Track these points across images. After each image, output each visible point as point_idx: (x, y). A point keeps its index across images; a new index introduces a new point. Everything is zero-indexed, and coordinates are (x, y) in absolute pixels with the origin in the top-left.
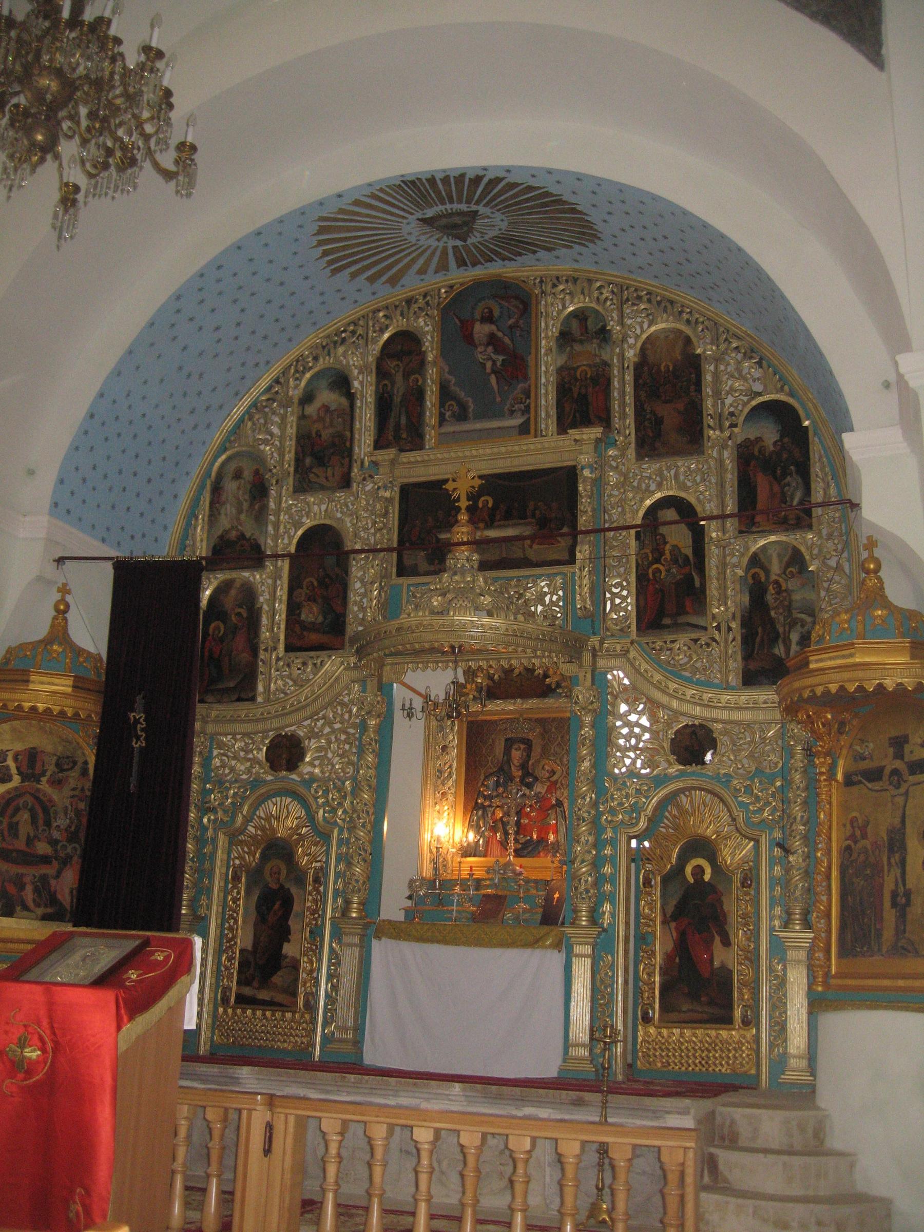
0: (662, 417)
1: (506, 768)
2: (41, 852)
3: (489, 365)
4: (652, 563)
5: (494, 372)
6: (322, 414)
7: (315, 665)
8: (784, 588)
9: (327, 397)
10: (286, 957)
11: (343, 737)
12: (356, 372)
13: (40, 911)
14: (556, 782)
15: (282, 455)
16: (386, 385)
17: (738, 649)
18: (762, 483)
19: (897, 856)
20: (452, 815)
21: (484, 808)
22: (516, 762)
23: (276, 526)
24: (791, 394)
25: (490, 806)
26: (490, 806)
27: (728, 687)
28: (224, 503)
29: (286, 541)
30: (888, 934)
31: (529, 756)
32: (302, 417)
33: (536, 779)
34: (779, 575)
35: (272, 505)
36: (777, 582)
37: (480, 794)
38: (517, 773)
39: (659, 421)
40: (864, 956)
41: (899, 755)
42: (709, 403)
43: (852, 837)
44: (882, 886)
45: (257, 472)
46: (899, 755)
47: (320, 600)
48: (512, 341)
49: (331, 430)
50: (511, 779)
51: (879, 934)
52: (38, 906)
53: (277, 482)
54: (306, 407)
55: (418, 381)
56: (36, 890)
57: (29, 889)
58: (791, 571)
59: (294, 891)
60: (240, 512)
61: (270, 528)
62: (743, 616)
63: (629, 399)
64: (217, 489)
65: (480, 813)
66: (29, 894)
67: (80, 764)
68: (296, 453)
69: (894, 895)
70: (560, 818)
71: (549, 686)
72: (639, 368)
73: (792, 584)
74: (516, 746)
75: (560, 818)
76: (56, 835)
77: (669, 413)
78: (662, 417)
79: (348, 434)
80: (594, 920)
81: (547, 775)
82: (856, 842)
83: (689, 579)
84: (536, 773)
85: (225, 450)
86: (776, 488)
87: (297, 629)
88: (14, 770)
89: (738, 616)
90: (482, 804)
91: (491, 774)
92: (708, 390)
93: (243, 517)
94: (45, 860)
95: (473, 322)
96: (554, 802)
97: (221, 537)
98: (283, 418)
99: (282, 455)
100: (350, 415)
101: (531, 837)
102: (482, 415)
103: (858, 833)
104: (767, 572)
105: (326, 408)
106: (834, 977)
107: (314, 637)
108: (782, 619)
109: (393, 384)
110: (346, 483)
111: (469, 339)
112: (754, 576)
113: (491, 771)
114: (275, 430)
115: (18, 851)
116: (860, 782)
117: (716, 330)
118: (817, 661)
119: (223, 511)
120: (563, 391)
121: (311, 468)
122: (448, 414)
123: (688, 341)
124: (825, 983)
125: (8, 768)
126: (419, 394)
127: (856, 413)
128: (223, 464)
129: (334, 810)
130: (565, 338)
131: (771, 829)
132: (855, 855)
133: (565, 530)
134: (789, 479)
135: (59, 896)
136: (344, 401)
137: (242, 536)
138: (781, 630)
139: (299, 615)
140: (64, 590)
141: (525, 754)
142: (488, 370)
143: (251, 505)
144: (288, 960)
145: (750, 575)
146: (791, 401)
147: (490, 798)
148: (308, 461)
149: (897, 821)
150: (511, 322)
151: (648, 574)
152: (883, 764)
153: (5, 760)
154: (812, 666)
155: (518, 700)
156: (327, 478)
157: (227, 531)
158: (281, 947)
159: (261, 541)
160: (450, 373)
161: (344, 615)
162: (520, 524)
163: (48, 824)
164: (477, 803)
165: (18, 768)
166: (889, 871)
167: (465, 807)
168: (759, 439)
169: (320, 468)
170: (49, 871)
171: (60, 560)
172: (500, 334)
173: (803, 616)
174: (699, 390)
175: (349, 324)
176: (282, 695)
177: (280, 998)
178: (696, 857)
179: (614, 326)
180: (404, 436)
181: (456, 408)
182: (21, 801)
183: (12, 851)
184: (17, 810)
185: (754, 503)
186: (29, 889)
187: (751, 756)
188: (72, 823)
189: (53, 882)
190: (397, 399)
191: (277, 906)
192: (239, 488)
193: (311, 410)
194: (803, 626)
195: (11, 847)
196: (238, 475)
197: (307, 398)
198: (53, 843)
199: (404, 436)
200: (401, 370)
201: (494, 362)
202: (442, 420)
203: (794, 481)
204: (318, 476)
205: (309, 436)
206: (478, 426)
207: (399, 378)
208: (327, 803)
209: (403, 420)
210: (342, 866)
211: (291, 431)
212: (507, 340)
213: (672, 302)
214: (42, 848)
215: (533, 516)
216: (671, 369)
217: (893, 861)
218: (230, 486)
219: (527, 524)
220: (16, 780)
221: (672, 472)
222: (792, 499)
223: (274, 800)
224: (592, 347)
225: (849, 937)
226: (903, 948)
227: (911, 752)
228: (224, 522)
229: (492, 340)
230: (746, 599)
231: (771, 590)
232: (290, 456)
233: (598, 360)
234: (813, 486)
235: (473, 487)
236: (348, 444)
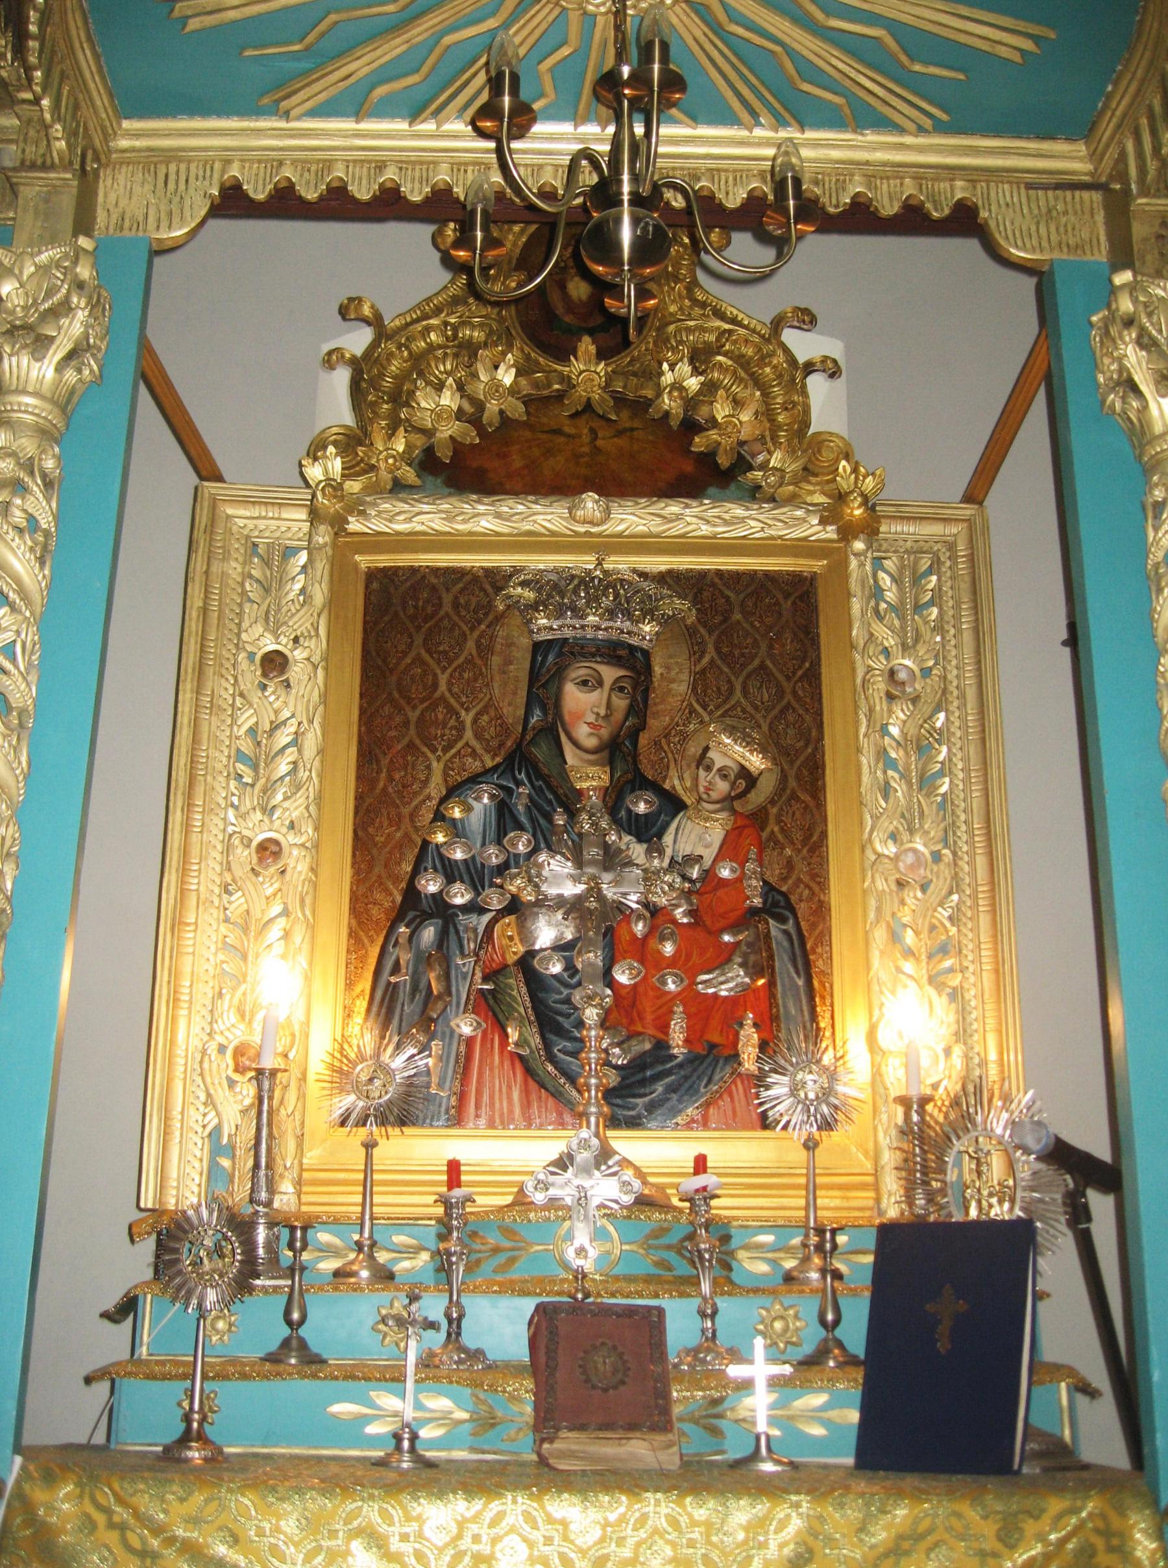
1: (541, 753)
14: (758, 818)
20: (298, 937)
21: (440, 908)
22: (583, 732)
26: (473, 908)
31: (639, 709)
33: (673, 805)
50: (571, 801)
65: (429, 934)
70: (783, 963)
71: (708, 458)
74: (579, 671)
75: (783, 963)
81: (723, 786)
84: (674, 783)
90: (438, 898)
91: (474, 780)
96: (757, 901)
101: (662, 1045)
113: (474, 766)
141: (621, 703)
155: (590, 503)
164: (412, 893)
167: (359, 906)
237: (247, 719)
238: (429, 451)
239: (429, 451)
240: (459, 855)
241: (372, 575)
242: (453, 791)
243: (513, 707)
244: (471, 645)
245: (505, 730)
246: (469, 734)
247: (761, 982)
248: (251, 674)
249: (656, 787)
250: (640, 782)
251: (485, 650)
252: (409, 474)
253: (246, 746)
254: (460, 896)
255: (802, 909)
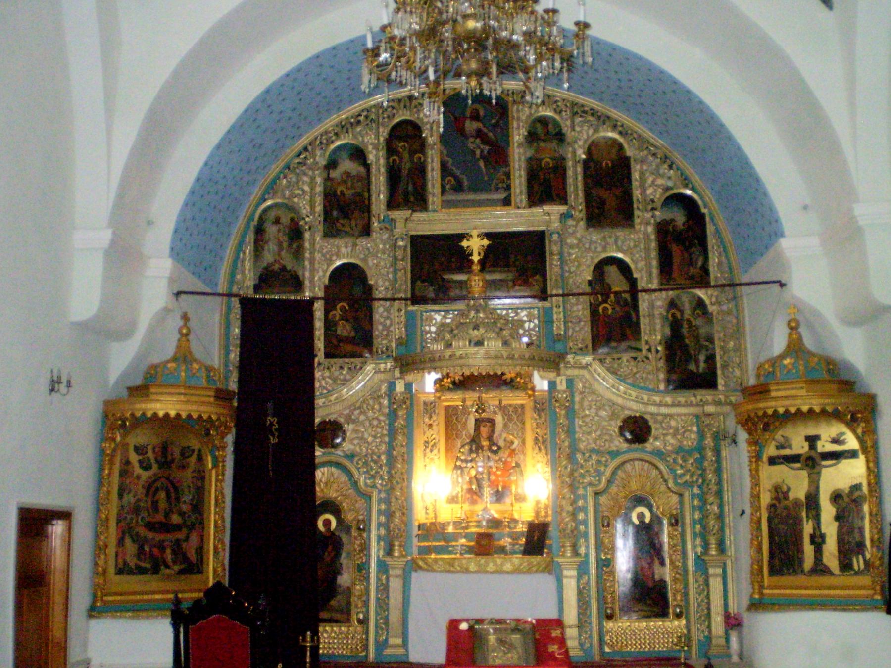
0: (605, 200)
2: (175, 522)
3: (478, 152)
4: (601, 303)
5: (482, 157)
6: (345, 177)
7: (350, 368)
8: (694, 324)
9: (347, 165)
10: (340, 586)
11: (375, 422)
12: (370, 148)
13: (177, 568)
14: (514, 450)
15: (312, 207)
16: (394, 161)
17: (661, 364)
18: (675, 249)
19: (814, 512)
21: (460, 468)
23: (312, 261)
24: (693, 189)
25: (466, 467)
26: (466, 467)
27: (657, 391)
28: (267, 242)
29: (321, 273)
30: (809, 561)
31: (493, 431)
32: (328, 179)
34: (689, 315)
35: (307, 245)
36: (688, 320)
37: (458, 458)
38: (485, 443)
39: (603, 203)
40: (790, 574)
41: (813, 447)
42: (636, 193)
43: (777, 498)
44: (801, 531)
45: (292, 219)
46: (813, 447)
47: (352, 320)
48: (495, 136)
49: (353, 191)
50: (482, 448)
51: (801, 561)
52: (175, 562)
53: (310, 228)
54: (331, 171)
55: (420, 158)
56: (174, 552)
57: (168, 551)
58: (698, 314)
59: (344, 538)
60: (281, 249)
61: (307, 263)
62: (666, 342)
63: (580, 186)
64: (260, 231)
65: (459, 472)
66: (169, 555)
67: (196, 453)
68: (325, 206)
69: (812, 537)
72: (586, 163)
73: (698, 322)
74: (484, 424)
76: (185, 508)
77: (610, 198)
78: (605, 200)
79: (366, 195)
80: (576, 553)
82: (780, 503)
83: (628, 317)
85: (265, 200)
86: (686, 255)
87: (335, 342)
88: (153, 461)
89: (663, 342)
92: (635, 184)
93: (283, 253)
94: (178, 527)
95: (465, 118)
96: (514, 464)
97: (266, 269)
98: (313, 179)
99: (312, 207)
100: (366, 180)
102: (474, 189)
103: (781, 496)
104: (682, 312)
105: (348, 174)
106: (769, 587)
107: (349, 348)
108: (693, 344)
109: (401, 159)
110: (366, 231)
111: (462, 131)
112: (673, 315)
114: (307, 188)
115: (160, 523)
116: (782, 463)
117: (644, 143)
118: (776, 390)
119: (266, 248)
120: (533, 175)
121: (337, 220)
122: (448, 187)
123: (621, 147)
124: (761, 594)
125: (148, 459)
126: (420, 170)
127: (787, 225)
128: (265, 211)
129: (373, 477)
130: (532, 137)
131: (692, 487)
132: (779, 511)
133: (538, 277)
134: (693, 249)
135: (189, 555)
136: (362, 169)
137: (283, 269)
138: (693, 352)
139: (336, 331)
140: (185, 317)
142: (478, 156)
143: (290, 245)
144: (342, 589)
145: (670, 316)
146: (695, 196)
147: (466, 461)
148: (335, 213)
149: (813, 489)
150: (493, 121)
151: (598, 310)
152: (801, 451)
153: (147, 452)
154: (773, 394)
156: (351, 228)
157: (269, 265)
158: (335, 579)
159: (300, 273)
160: (448, 156)
161: (371, 331)
162: (505, 271)
163: (178, 499)
164: (456, 465)
165: (156, 459)
166: (807, 521)
167: (447, 466)
168: (672, 220)
169: (346, 220)
170: (181, 536)
171: (178, 294)
172: (485, 130)
173: (707, 344)
174: (630, 182)
175: (363, 111)
176: (325, 392)
177: (338, 616)
178: (640, 506)
179: (566, 130)
180: (412, 199)
181: (453, 182)
182: (159, 484)
183: (155, 523)
184: (157, 490)
185: (670, 264)
186: (168, 551)
187: (674, 435)
188: (194, 497)
189: (184, 545)
190: (405, 172)
191: (330, 548)
192: (279, 231)
193: (335, 174)
194: (707, 350)
195: (155, 520)
196: (277, 221)
197: (332, 164)
198: (182, 514)
199: (412, 199)
200: (407, 149)
201: (482, 152)
202: (443, 191)
203: (696, 250)
204: (343, 225)
205: (335, 195)
206: (471, 197)
207: (406, 155)
208: (367, 472)
209: (410, 188)
210: (383, 519)
211: (319, 189)
212: (490, 134)
213: (608, 117)
214: (176, 519)
215: (515, 266)
216: (610, 165)
217: (810, 515)
218: (271, 230)
219: (509, 271)
220: (155, 467)
221: (613, 239)
222: (696, 263)
223: (322, 469)
224: (553, 145)
225: (777, 562)
226: (821, 570)
227: (823, 446)
228: (268, 257)
229: (479, 134)
230: (668, 331)
231: (685, 325)
232: (319, 208)
233: (557, 155)
234: (710, 255)
235: (483, 246)
236: (367, 202)
237: (426, 436)
238: (454, 381)
239: (454, 381)
240: (462, 458)
241: (447, 408)
242: (463, 446)
243: (472, 432)
244: (464, 420)
245: (470, 435)
246: (464, 436)
247: (515, 478)
248: (426, 428)
249: (497, 446)
250: (494, 444)
251: (466, 420)
252: (451, 386)
253: (426, 440)
254: (464, 465)
255: (522, 466)
